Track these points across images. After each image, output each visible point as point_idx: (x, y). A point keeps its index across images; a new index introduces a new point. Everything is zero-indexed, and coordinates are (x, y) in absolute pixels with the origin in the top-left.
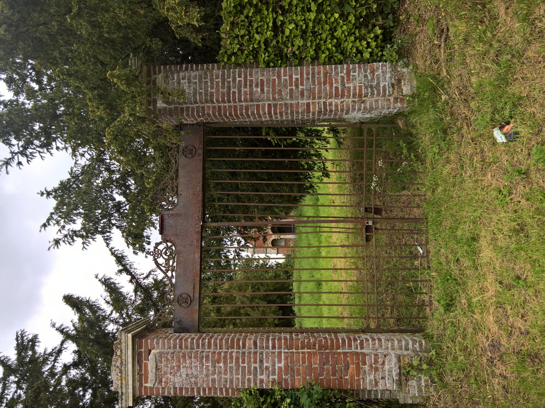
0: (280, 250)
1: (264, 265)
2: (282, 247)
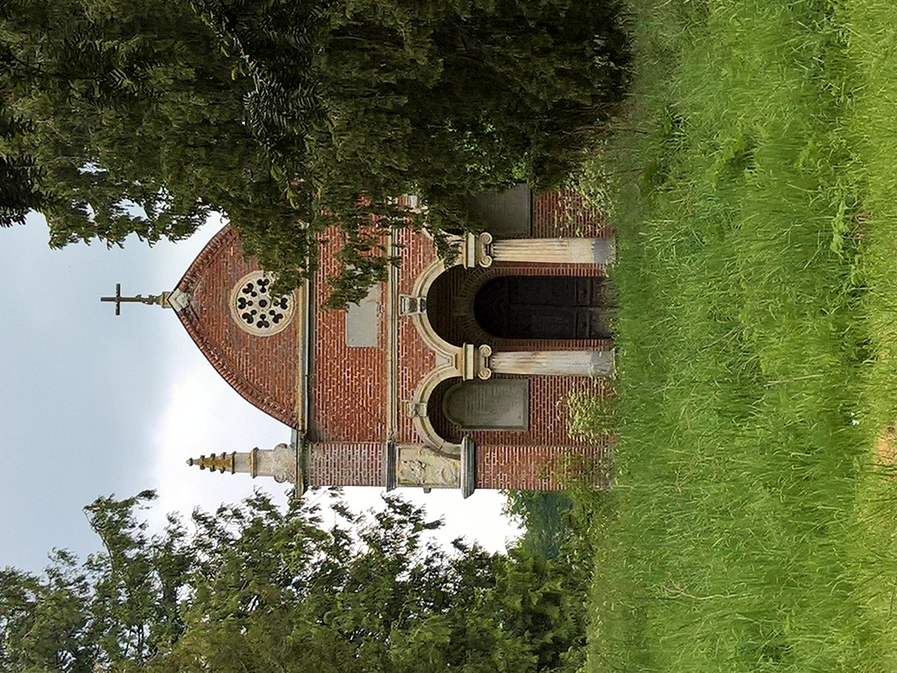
0: (491, 456)
1: (381, 564)
2: (510, 438)
